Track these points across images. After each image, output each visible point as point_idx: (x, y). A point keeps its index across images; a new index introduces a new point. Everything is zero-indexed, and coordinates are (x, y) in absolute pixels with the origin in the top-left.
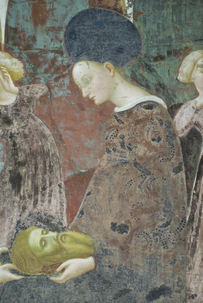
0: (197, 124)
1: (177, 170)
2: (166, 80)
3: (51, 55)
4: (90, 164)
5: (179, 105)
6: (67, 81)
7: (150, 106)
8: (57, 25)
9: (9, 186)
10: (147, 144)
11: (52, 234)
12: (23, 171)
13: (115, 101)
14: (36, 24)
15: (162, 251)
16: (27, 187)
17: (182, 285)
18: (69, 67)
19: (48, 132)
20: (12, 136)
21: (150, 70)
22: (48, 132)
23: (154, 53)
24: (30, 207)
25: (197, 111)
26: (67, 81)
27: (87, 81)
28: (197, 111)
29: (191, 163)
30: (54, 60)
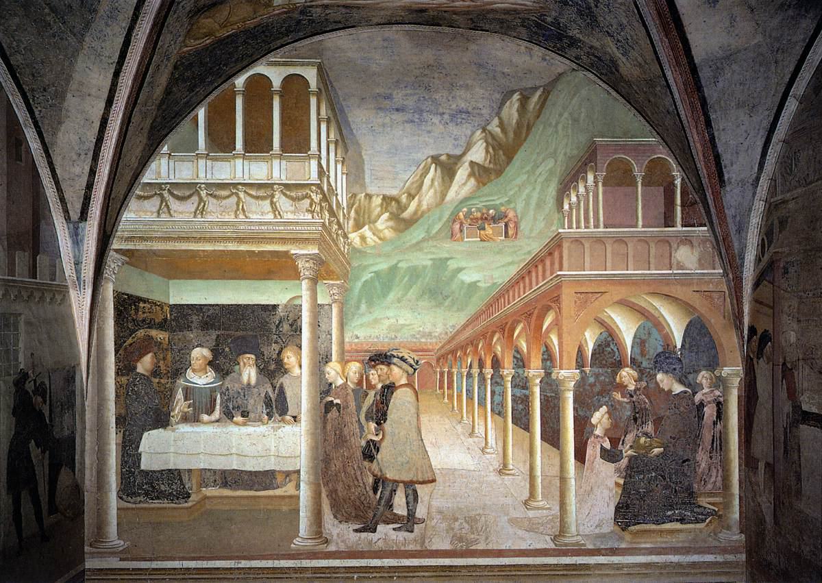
0: (703, 400)
1: (695, 417)
2: (692, 382)
3: (648, 370)
4: (662, 414)
5: (696, 393)
6: (654, 381)
7: (685, 392)
8: (650, 357)
9: (632, 421)
10: (684, 407)
11: (649, 439)
12: (637, 415)
13: (673, 390)
14: (642, 356)
15: (688, 446)
16: (639, 421)
17: (694, 457)
18: (655, 375)
19: (647, 401)
20: (633, 402)
21: (686, 377)
22: (647, 401)
23: (688, 371)
24: (640, 429)
25: (703, 395)
26: (654, 381)
27: (662, 381)
28: (703, 395)
29: (700, 415)
30: (649, 372)
